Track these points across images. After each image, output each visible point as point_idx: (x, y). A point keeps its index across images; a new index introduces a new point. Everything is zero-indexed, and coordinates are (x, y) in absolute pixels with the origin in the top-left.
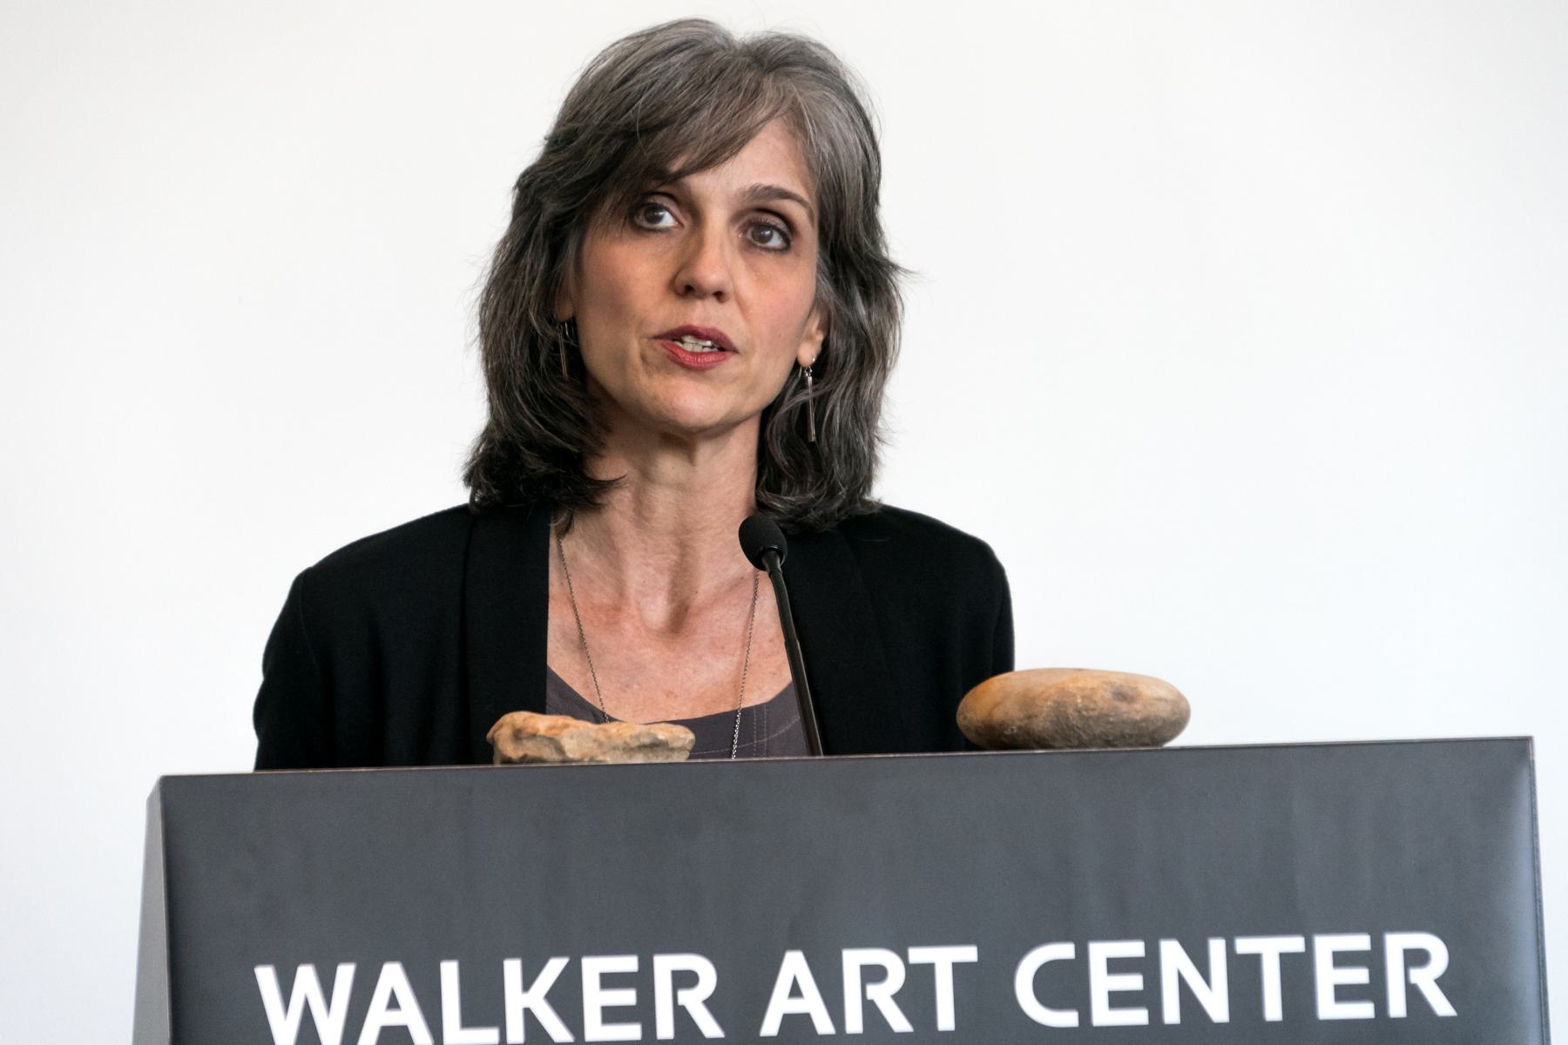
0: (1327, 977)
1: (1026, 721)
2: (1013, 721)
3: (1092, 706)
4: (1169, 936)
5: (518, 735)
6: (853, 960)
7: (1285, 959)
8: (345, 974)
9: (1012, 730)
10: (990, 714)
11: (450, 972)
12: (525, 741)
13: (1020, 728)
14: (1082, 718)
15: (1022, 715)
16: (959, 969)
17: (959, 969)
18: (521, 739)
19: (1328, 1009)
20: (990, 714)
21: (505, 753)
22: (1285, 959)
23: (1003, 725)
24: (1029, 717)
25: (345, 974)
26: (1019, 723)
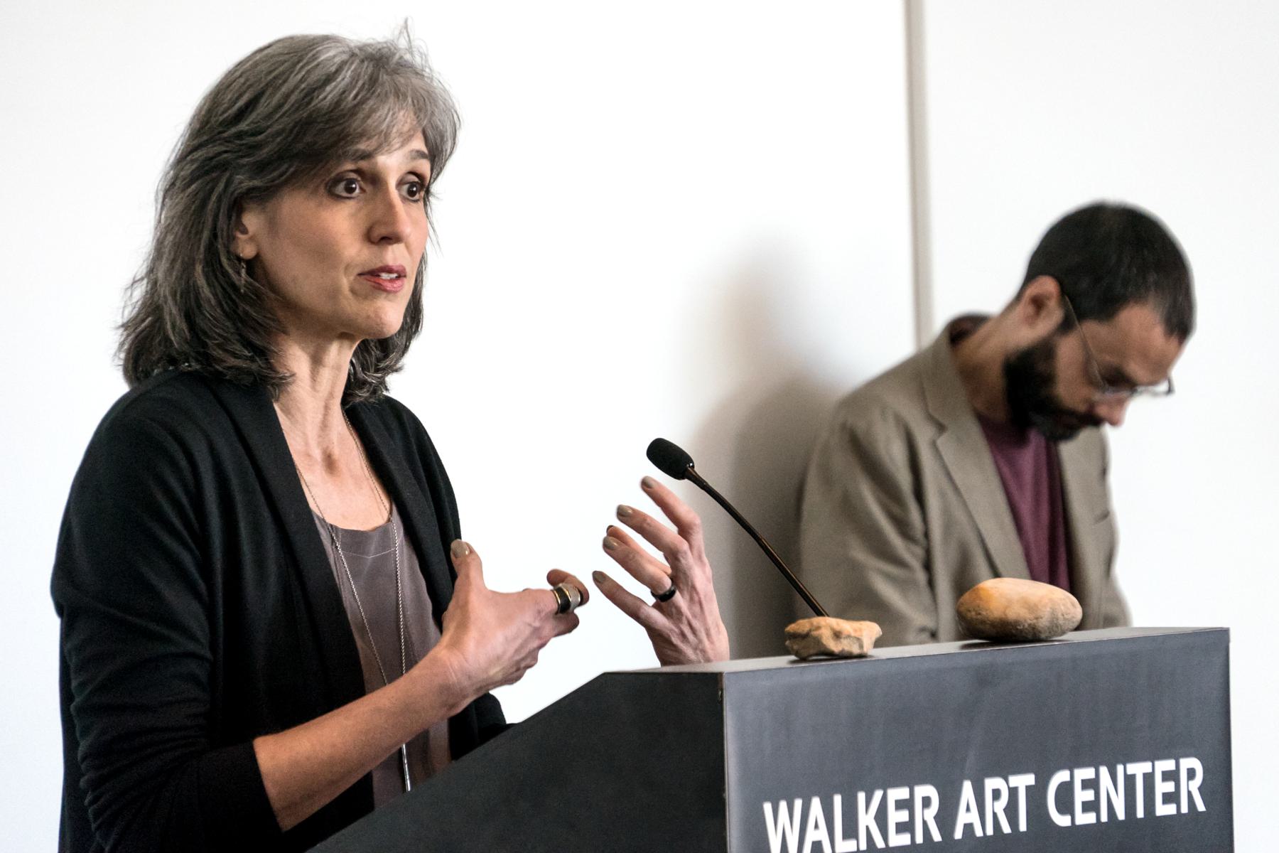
0: (1162, 787)
1: (1035, 621)
2: (1025, 621)
3: (1068, 612)
4: (1102, 764)
5: (837, 635)
6: (991, 783)
7: (1145, 775)
8: (798, 804)
9: (1024, 626)
10: (1004, 613)
11: (838, 800)
12: (842, 640)
13: (1030, 625)
14: (1065, 619)
15: (1032, 617)
16: (1028, 788)
17: (1028, 788)
18: (841, 638)
19: (1163, 810)
20: (1004, 613)
21: (828, 647)
22: (1145, 775)
23: (1017, 623)
24: (1037, 618)
25: (798, 804)
26: (1029, 622)
